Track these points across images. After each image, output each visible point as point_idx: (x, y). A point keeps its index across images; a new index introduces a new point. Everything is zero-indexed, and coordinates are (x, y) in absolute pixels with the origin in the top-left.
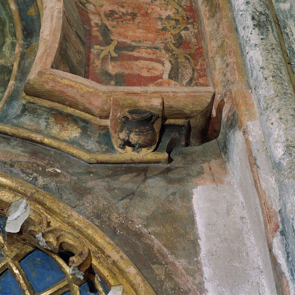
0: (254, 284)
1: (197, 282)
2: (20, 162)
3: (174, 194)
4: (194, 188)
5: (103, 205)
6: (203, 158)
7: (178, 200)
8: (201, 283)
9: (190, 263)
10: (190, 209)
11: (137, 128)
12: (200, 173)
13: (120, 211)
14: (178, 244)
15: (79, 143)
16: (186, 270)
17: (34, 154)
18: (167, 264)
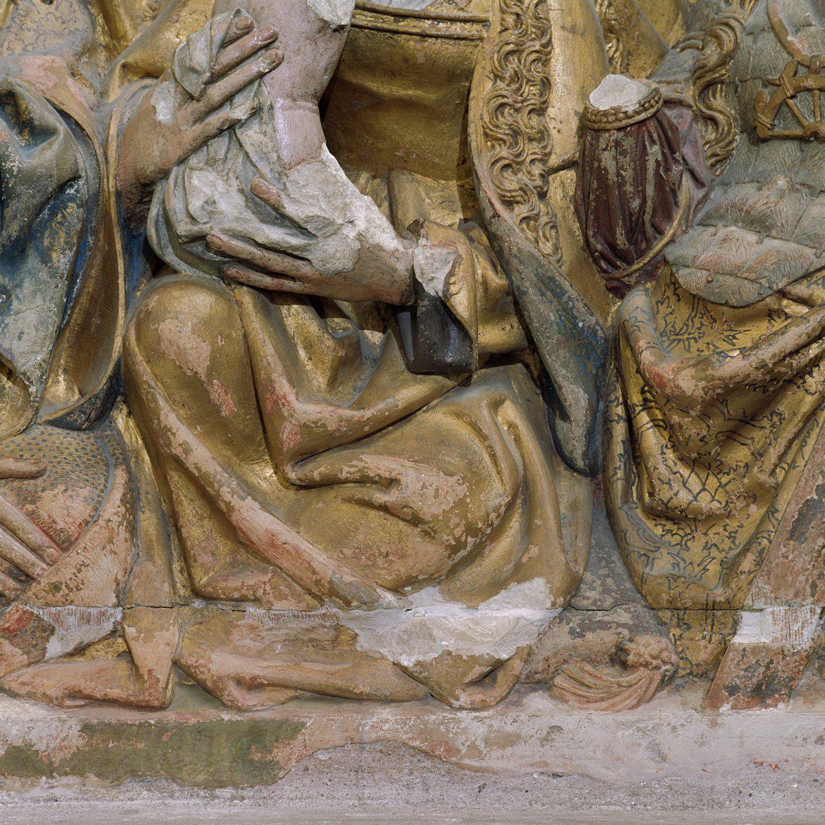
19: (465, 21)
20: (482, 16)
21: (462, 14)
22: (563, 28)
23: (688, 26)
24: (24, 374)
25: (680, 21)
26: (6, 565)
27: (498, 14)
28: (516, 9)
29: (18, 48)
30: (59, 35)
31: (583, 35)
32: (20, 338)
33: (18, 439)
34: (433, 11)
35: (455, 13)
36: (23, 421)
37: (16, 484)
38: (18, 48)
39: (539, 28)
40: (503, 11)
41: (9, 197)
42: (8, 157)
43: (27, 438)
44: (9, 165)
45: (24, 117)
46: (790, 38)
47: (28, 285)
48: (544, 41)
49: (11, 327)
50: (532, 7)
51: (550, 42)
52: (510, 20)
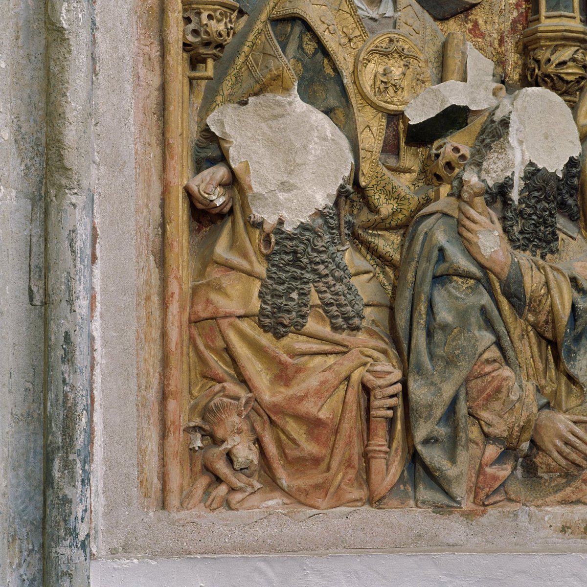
24: (583, 383)
26: (583, 455)
29: (568, 260)
30: (580, 253)
32: (581, 370)
33: (579, 408)
36: (580, 401)
37: (584, 425)
38: (568, 260)
41: (579, 318)
42: (579, 302)
43: (583, 407)
44: (579, 306)
45: (580, 287)
47: (582, 351)
49: (577, 366)
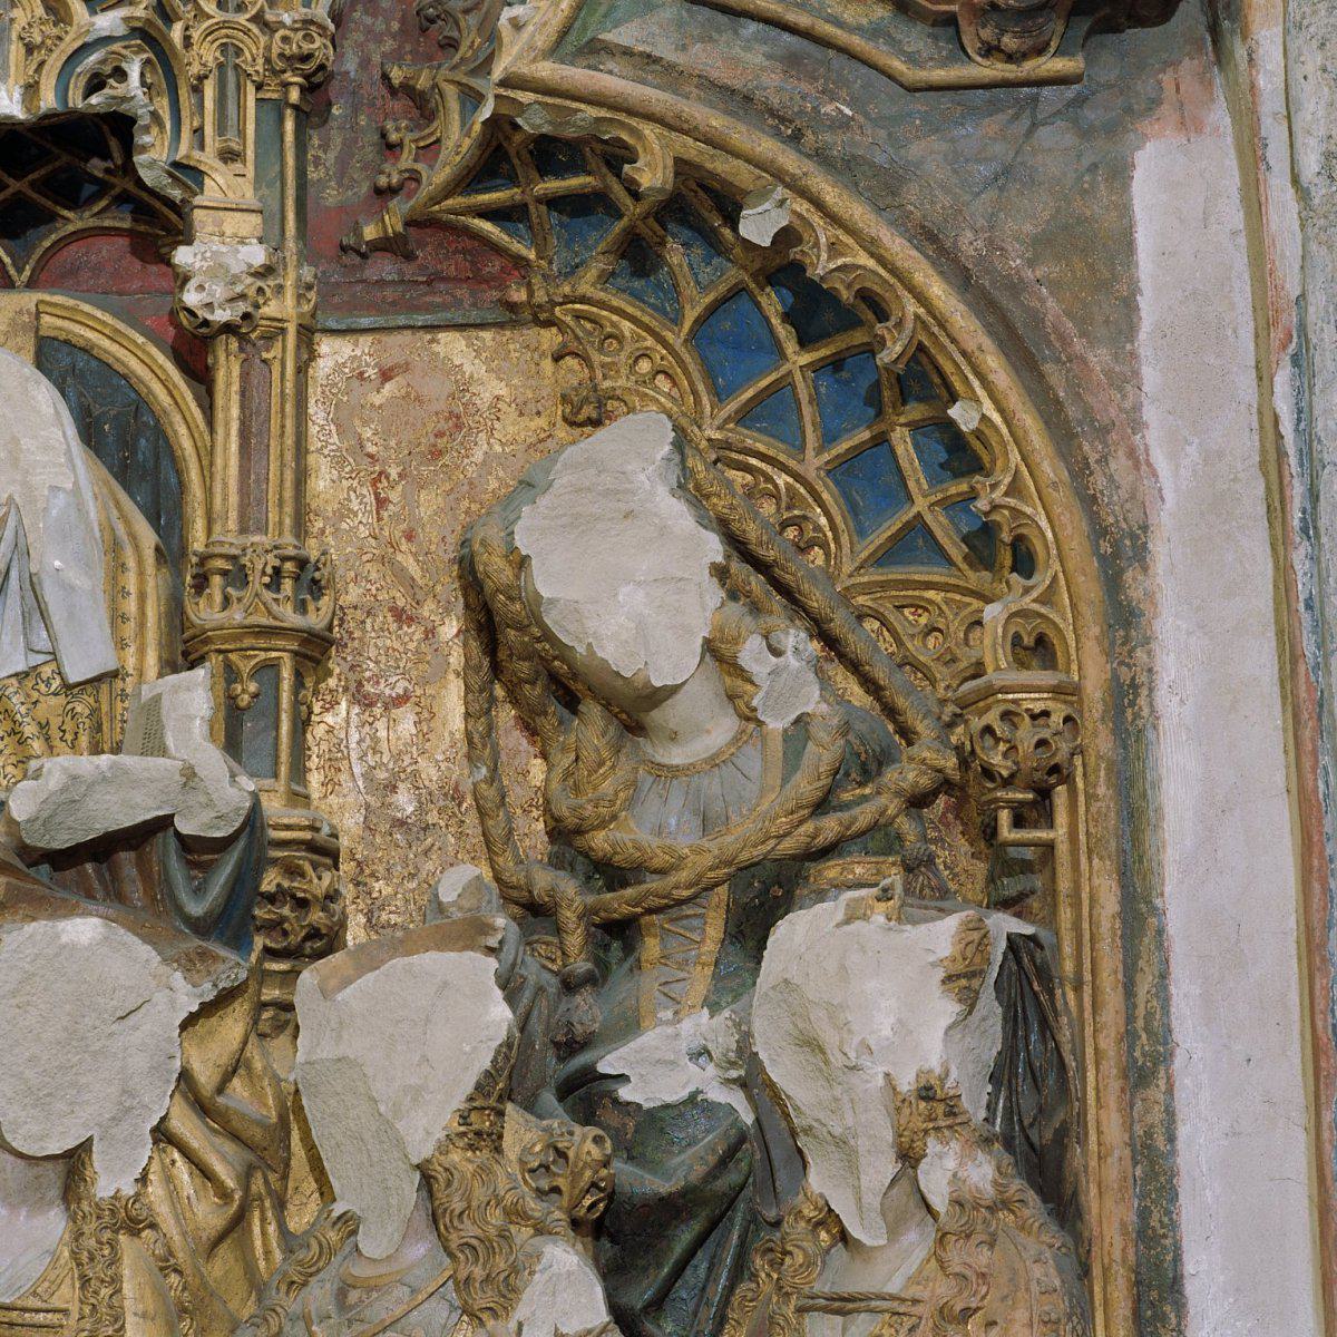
0: (1242, 407)
1: (1127, 405)
2: (765, 89)
3: (1093, 168)
4: (1139, 148)
5: (943, 208)
6: (1165, 56)
7: (1102, 187)
8: (1137, 408)
9: (1116, 356)
10: (1125, 210)
11: (1016, 25)
12: (1155, 102)
13: (978, 225)
14: (1096, 309)
15: (890, 36)
16: (1108, 373)
17: (792, 62)
18: (1070, 361)
19: (48, 1311)
20: (64, 1306)
21: (44, 1306)
22: (135, 1314)
23: (259, 1300)
25: (253, 1298)
27: (77, 1304)
28: (93, 1301)
31: (153, 1319)
34: (20, 1303)
35: (39, 1304)
39: (112, 1316)
40: (81, 1302)
46: (314, 1328)
48: (116, 1327)
50: (107, 1297)
51: (123, 1325)
52: (87, 1310)
